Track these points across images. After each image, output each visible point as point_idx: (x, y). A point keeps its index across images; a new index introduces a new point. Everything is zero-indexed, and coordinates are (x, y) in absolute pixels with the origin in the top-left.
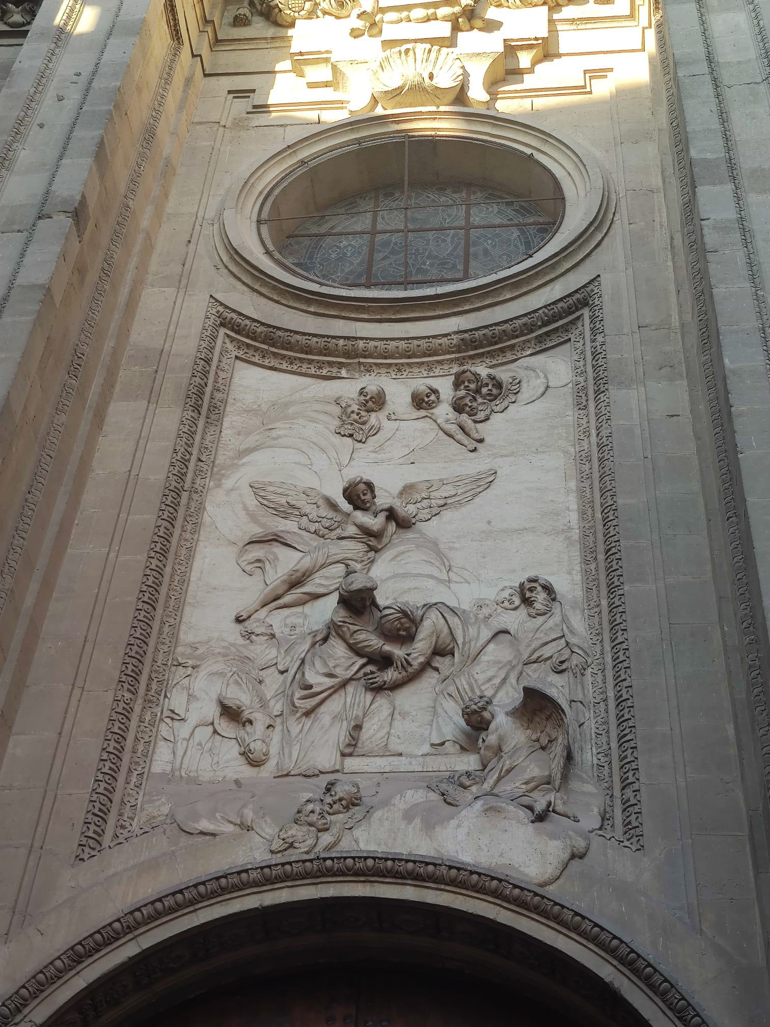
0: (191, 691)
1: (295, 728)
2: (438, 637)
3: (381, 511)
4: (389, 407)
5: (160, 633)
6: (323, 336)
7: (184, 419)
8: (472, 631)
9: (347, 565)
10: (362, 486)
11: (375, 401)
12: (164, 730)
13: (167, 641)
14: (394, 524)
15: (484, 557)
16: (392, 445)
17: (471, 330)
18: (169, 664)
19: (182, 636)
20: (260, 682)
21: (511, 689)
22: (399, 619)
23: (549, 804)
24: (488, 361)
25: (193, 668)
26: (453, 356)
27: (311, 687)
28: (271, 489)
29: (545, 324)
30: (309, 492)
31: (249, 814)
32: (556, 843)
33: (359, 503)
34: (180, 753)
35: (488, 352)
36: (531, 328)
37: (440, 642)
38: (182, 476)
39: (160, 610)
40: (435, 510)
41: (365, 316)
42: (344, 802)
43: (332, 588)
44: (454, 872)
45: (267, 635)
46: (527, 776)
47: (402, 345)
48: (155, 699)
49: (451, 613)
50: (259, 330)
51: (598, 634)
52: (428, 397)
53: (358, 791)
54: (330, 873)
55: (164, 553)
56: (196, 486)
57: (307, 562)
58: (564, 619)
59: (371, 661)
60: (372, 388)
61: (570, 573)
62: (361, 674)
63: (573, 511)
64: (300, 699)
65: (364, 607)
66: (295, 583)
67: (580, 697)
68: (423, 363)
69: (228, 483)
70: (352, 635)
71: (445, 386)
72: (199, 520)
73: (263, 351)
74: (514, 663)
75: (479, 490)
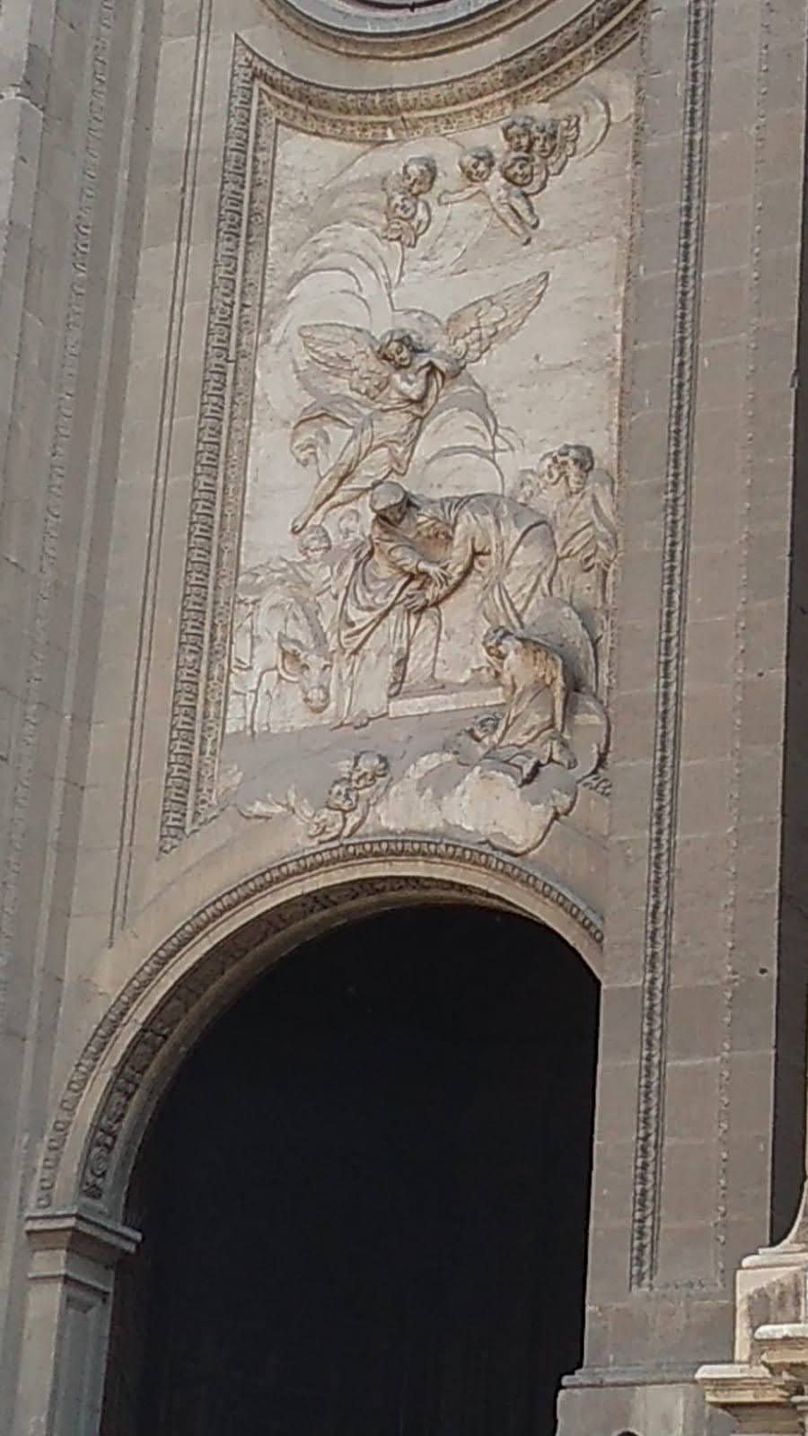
12: (234, 686)
16: (443, 244)
26: (504, 93)
27: (352, 624)
39: (215, 539)
46: (527, 726)
47: (444, 91)
52: (475, 166)
62: (403, 596)
74: (545, 564)
75: (529, 308)
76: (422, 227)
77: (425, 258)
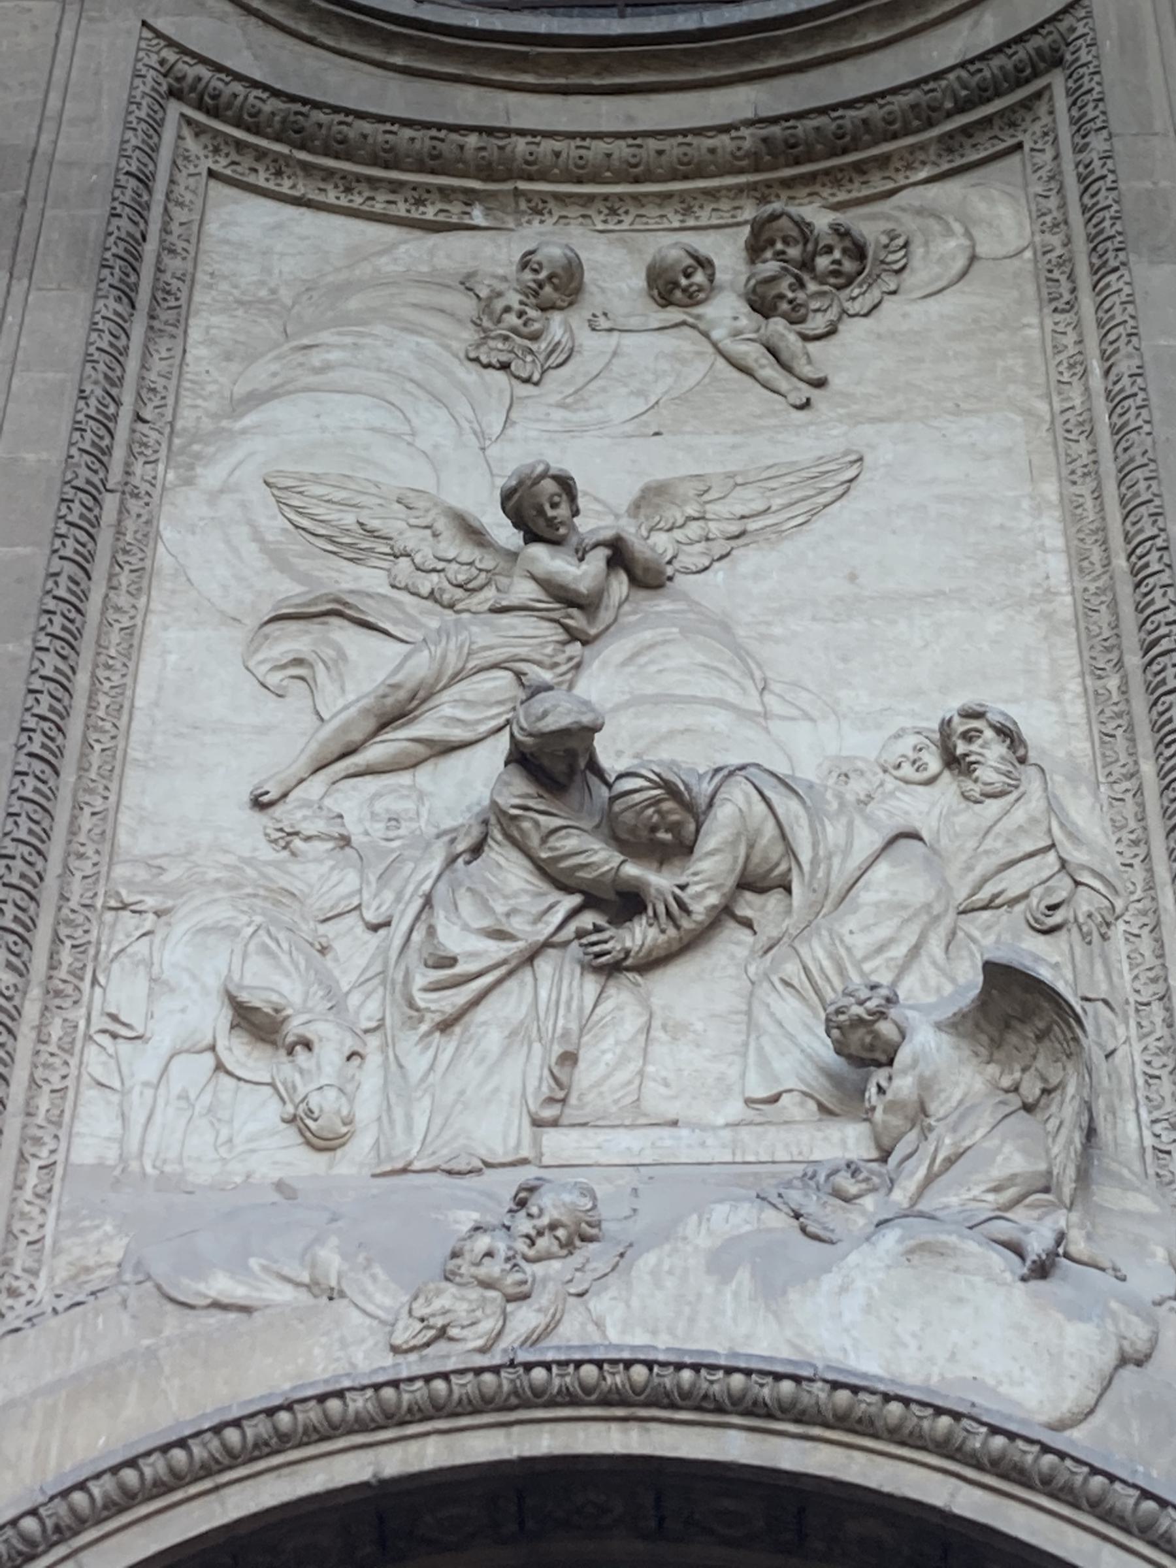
0: (156, 970)
1: (417, 1063)
2: (751, 846)
3: (596, 545)
4: (594, 298)
5: (73, 831)
6: (427, 125)
7: (98, 318)
8: (833, 833)
9: (519, 675)
10: (549, 486)
11: (561, 286)
12: (95, 1062)
13: (89, 851)
14: (624, 577)
15: (845, 659)
17: (787, 117)
18: (99, 903)
19: (123, 838)
20: (323, 950)
21: (931, 971)
22: (656, 802)
23: (1061, 1237)
24: (826, 192)
25: (158, 914)
26: (742, 179)
27: (452, 961)
28: (319, 490)
29: (962, 107)
30: (412, 499)
31: (331, 1260)
32: (1089, 1329)
33: (540, 527)
34: (138, 1117)
35: (827, 172)
36: (928, 116)
37: (756, 859)
38: (101, 456)
39: (69, 776)
40: (719, 548)
41: (530, 79)
42: (561, 1233)
43: (483, 729)
44: (843, 1396)
45: (331, 838)
46: (997, 1173)
48: (69, 989)
49: (782, 789)
50: (267, 108)
51: (1136, 843)
53: (594, 1207)
54: (539, 1398)
55: (70, 640)
56: (136, 481)
57: (420, 666)
58: (1052, 807)
59: (591, 902)
60: (553, 252)
61: (1056, 699)
63: (1054, 551)
64: (426, 990)
65: (572, 771)
66: (391, 717)
67: (1103, 990)
68: (669, 196)
69: (211, 476)
70: (544, 840)
71: (726, 251)
72: (148, 563)
73: (277, 157)
74: (937, 909)
75: (823, 499)
76: (555, 360)
77: (562, 405)
